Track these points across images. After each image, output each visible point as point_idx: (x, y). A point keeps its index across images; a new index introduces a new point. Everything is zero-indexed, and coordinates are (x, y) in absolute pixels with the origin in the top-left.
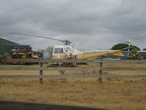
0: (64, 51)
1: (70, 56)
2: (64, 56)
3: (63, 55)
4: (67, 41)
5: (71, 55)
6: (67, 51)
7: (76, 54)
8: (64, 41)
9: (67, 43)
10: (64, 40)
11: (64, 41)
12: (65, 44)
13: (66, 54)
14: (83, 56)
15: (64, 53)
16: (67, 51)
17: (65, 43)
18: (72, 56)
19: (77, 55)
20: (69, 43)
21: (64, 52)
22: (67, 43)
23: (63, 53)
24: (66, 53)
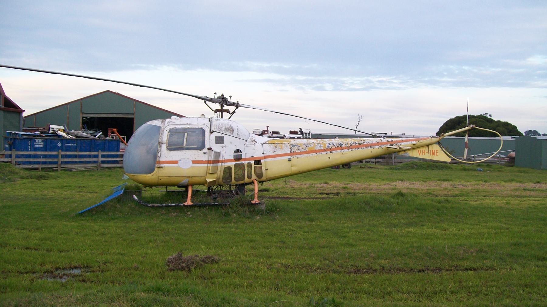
0: (210, 140)
1: (234, 163)
2: (208, 162)
3: (205, 158)
4: (223, 100)
5: (238, 158)
6: (220, 140)
7: (258, 154)
8: (211, 100)
9: (226, 107)
10: (212, 96)
11: (211, 100)
12: (216, 111)
13: (218, 154)
14: (289, 160)
15: (210, 149)
16: (220, 140)
17: (217, 106)
18: (245, 159)
19: (265, 157)
20: (232, 109)
21: (207, 146)
22: (226, 107)
23: (205, 150)
24: (217, 148)
